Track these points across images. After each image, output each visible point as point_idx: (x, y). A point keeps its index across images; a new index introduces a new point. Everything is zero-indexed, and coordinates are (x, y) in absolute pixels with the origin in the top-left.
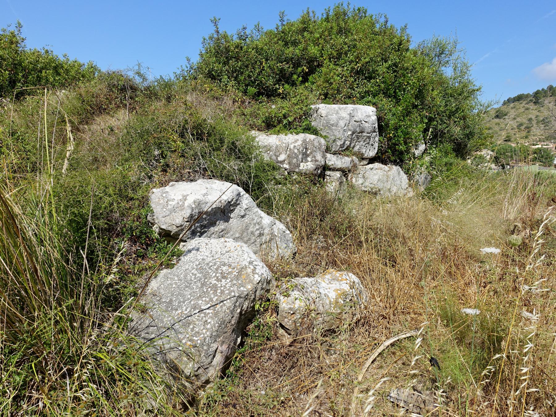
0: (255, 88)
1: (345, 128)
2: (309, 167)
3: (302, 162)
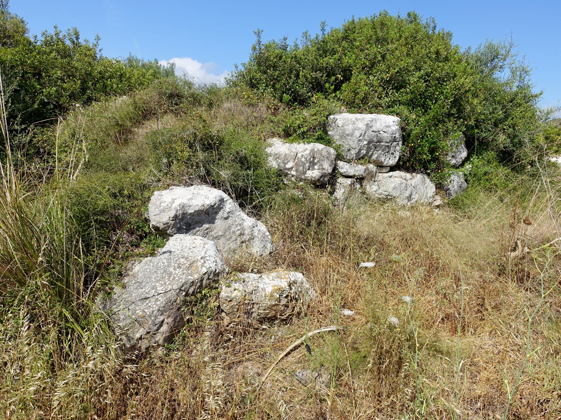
0: (290, 95)
1: (361, 138)
2: (314, 175)
3: (309, 169)
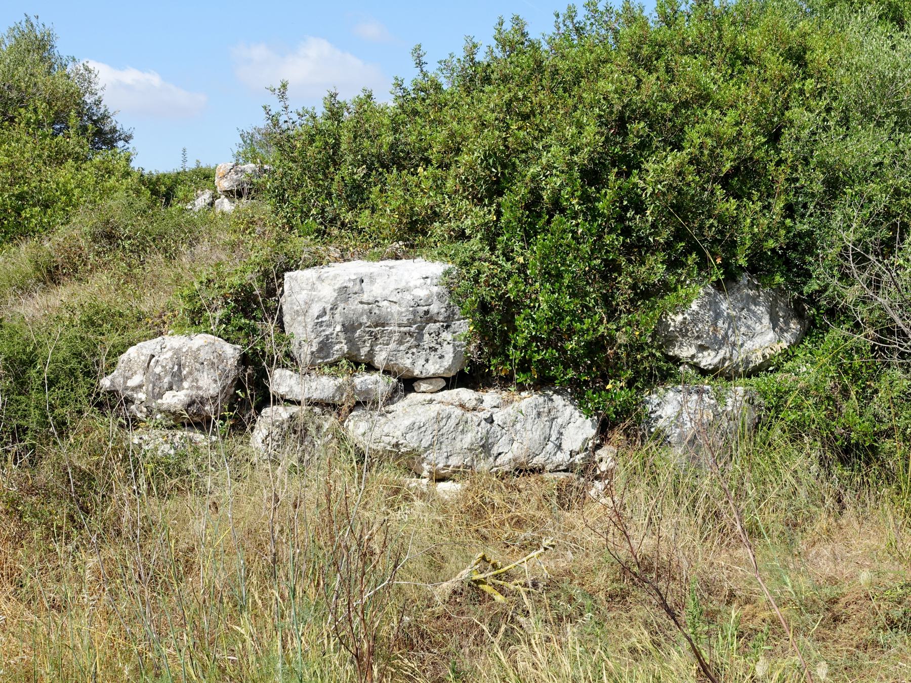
3: (171, 388)
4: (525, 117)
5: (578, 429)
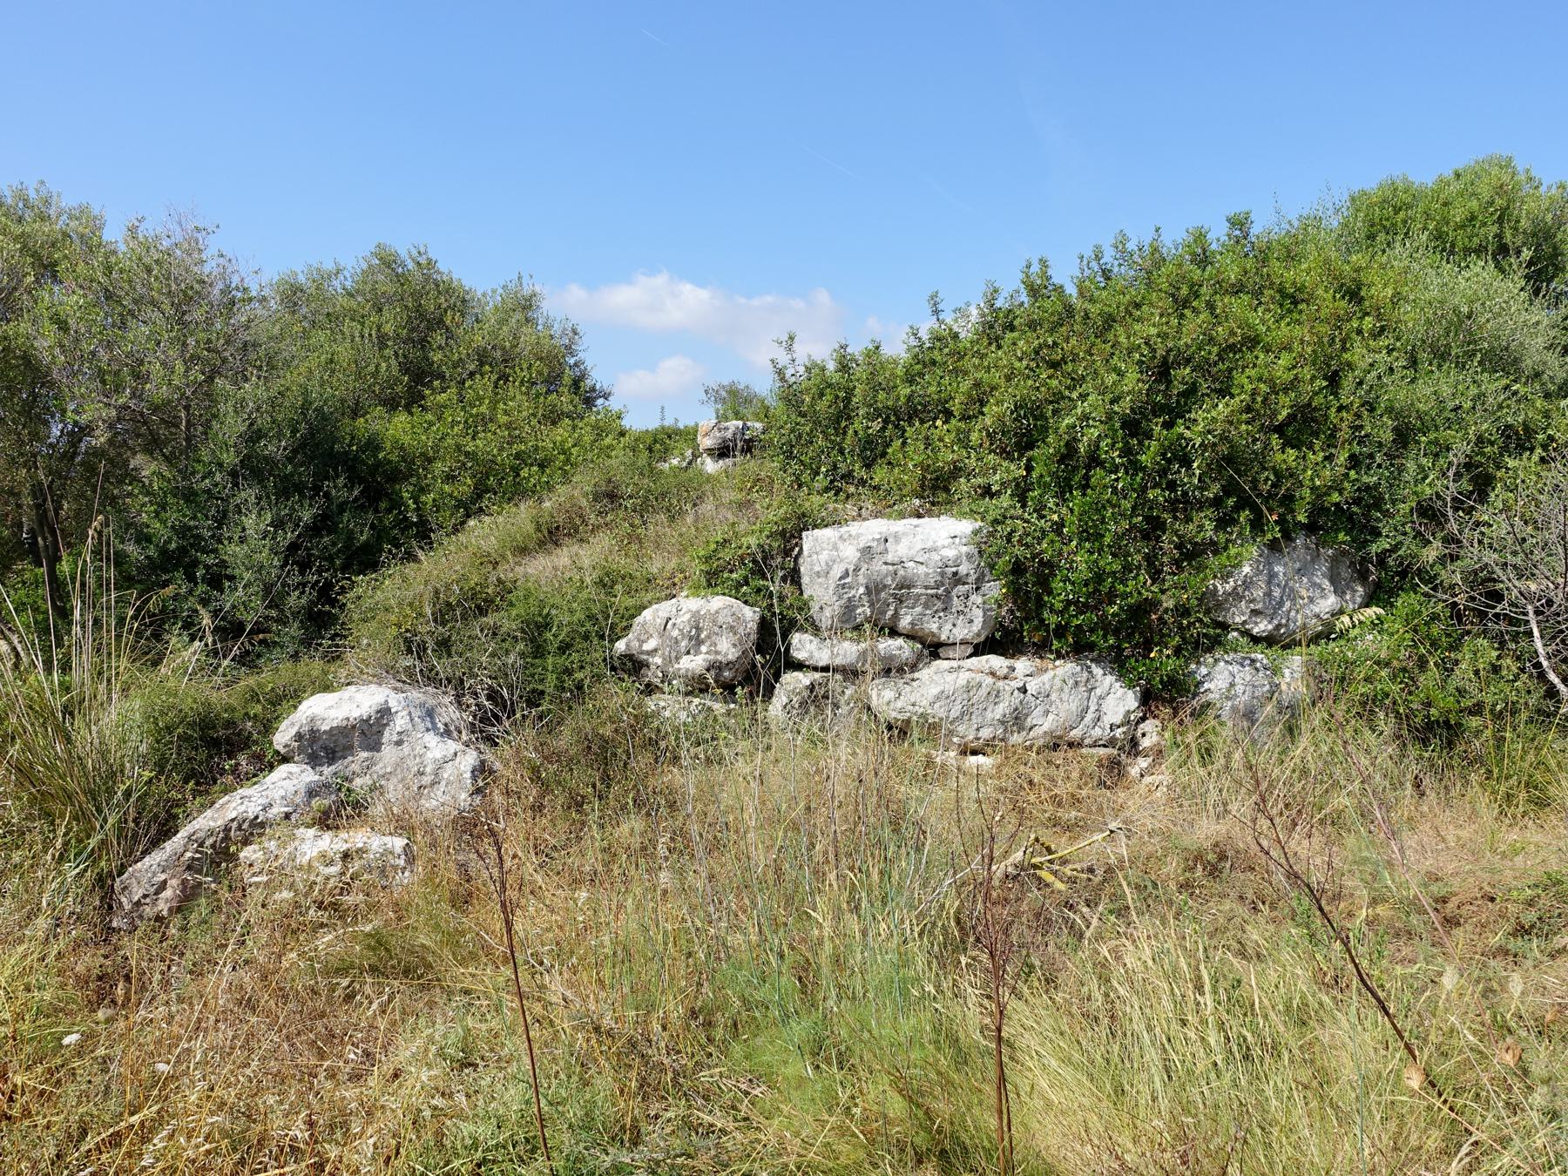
2: (691, 666)
4: (1054, 365)
5: (1117, 700)
